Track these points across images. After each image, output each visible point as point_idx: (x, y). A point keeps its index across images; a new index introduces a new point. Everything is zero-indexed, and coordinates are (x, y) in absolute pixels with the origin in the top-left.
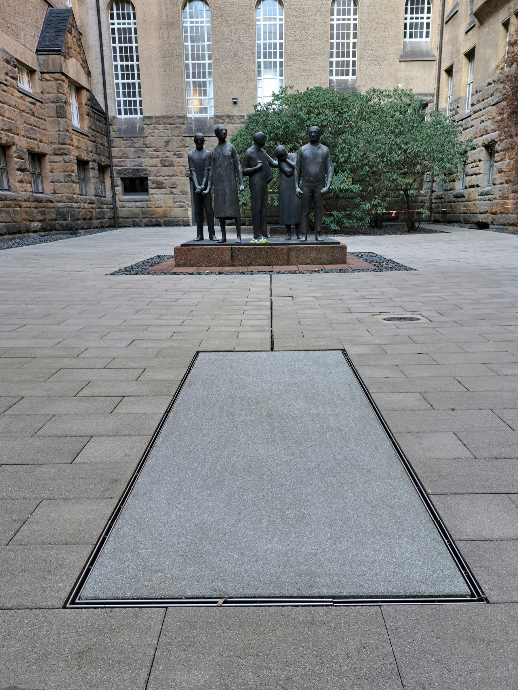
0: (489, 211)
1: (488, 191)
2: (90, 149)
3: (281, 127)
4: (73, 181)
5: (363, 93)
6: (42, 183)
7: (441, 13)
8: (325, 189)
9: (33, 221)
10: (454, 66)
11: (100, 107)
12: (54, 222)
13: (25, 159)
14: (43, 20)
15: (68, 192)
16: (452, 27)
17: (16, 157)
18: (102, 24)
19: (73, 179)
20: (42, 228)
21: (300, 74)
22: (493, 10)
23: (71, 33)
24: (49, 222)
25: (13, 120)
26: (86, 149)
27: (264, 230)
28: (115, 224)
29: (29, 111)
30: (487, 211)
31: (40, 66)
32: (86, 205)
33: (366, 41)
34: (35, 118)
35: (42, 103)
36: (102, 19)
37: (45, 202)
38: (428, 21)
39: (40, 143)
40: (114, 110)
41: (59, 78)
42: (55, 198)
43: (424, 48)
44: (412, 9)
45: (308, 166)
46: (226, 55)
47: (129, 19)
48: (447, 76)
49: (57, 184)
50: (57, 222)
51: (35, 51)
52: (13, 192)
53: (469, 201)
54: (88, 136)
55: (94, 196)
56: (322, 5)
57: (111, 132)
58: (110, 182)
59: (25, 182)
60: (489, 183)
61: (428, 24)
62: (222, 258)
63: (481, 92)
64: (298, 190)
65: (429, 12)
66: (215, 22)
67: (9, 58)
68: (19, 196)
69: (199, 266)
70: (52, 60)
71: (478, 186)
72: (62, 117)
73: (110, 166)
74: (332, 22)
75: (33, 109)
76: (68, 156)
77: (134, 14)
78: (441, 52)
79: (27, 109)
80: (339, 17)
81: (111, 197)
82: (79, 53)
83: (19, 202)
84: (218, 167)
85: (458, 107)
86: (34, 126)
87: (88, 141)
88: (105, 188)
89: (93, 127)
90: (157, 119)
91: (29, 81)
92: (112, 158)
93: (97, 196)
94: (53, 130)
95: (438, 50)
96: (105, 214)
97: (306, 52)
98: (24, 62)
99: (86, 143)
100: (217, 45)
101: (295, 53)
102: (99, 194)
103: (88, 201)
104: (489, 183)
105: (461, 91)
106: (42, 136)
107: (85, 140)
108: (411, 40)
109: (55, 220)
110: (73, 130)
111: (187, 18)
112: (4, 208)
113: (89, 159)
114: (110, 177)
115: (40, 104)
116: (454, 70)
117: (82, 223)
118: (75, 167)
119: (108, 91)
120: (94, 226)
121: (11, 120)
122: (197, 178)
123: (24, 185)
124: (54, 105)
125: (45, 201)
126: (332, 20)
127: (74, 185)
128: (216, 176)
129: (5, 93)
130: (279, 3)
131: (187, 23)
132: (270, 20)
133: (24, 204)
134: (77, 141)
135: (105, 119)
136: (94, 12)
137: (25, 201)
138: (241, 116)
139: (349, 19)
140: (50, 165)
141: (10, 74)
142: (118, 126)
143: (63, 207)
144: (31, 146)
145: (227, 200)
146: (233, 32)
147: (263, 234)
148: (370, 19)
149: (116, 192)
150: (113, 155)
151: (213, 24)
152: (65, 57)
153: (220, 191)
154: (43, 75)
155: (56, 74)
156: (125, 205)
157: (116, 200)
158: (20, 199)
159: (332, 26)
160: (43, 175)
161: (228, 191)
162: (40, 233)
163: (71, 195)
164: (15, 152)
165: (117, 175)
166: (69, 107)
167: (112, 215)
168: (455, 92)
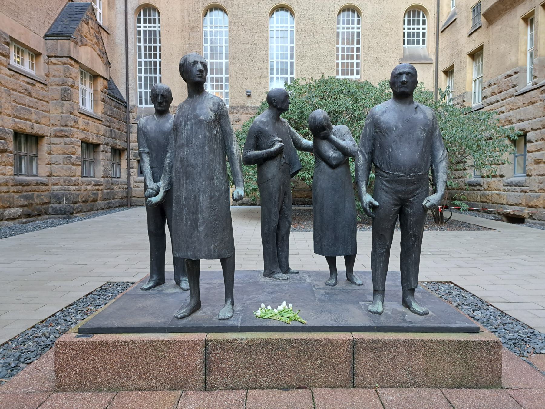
0: (523, 204)
1: (519, 182)
2: (102, 132)
3: (296, 112)
4: (73, 163)
5: (376, 85)
6: (37, 165)
7: (436, 24)
8: (433, 199)
9: (9, 207)
10: (455, 66)
11: (122, 97)
12: (46, 206)
13: (7, 139)
14: (60, 10)
15: (66, 174)
16: (449, 34)
18: (128, 26)
19: (72, 161)
20: (25, 214)
21: (309, 73)
22: (508, 7)
23: (87, 24)
24: (38, 207)
26: (95, 132)
27: (284, 260)
28: (128, 203)
29: (23, 91)
30: (520, 204)
31: (47, 51)
32: (89, 187)
33: (369, 46)
34: (32, 99)
35: (46, 85)
36: (129, 22)
38: (424, 31)
39: (35, 124)
40: (134, 100)
41: (66, 62)
42: (51, 181)
43: (422, 53)
44: (409, 21)
45: (394, 146)
46: (242, 55)
47: (155, 23)
48: (445, 76)
49: (55, 166)
50: (50, 205)
51: (43, 35)
53: (490, 191)
54: (101, 121)
55: (103, 177)
56: (329, 16)
57: (131, 119)
58: (126, 164)
59: (3, 164)
60: (514, 173)
61: (424, 34)
62: (181, 367)
63: (496, 85)
64: (367, 198)
65: (424, 23)
66: (233, 27)
69: (117, 391)
70: (61, 45)
71: (502, 176)
72: (66, 99)
73: (127, 149)
74: (338, 30)
75: (30, 89)
77: (159, 19)
78: (438, 56)
79: (21, 88)
80: (344, 26)
81: (125, 178)
82: (98, 44)
84: (182, 146)
85: (464, 101)
86: (29, 106)
87: (100, 126)
88: (120, 170)
89: (109, 113)
90: (175, 109)
91: (33, 64)
92: (130, 143)
93: (107, 177)
94: (55, 112)
95: (435, 55)
96: (116, 195)
97: (315, 54)
98: (23, 42)
99: (97, 127)
100: (234, 46)
101: (304, 54)
102: (109, 176)
103: (93, 183)
104: (514, 173)
105: (467, 87)
106: (40, 118)
107: (96, 124)
108: (409, 46)
109: (49, 203)
110: (80, 113)
111: (207, 24)
113: (99, 142)
114: (127, 159)
115: (42, 86)
116: (455, 69)
117: (81, 206)
118: (79, 150)
119: (130, 82)
120: (99, 207)
122: (152, 168)
124: (59, 88)
125: (35, 184)
126: (338, 28)
127: (74, 167)
128: (178, 165)
130: (291, 14)
131: (207, 27)
132: (282, 27)
134: (85, 124)
135: (126, 107)
136: (123, 16)
138: (254, 107)
139: (353, 28)
140: (47, 147)
142: (138, 114)
143: (58, 190)
144: (19, 126)
145: (201, 220)
146: (248, 36)
147: (281, 267)
148: (372, 27)
149: (131, 174)
150: (131, 139)
151: (230, 29)
152: (76, 43)
153: (186, 199)
154: (49, 59)
155: (64, 58)
156: (139, 186)
157: (130, 181)
159: (338, 33)
161: (204, 201)
162: (20, 220)
163: (69, 178)
165: (134, 158)
166: (77, 90)
167: (125, 195)
168: (459, 89)
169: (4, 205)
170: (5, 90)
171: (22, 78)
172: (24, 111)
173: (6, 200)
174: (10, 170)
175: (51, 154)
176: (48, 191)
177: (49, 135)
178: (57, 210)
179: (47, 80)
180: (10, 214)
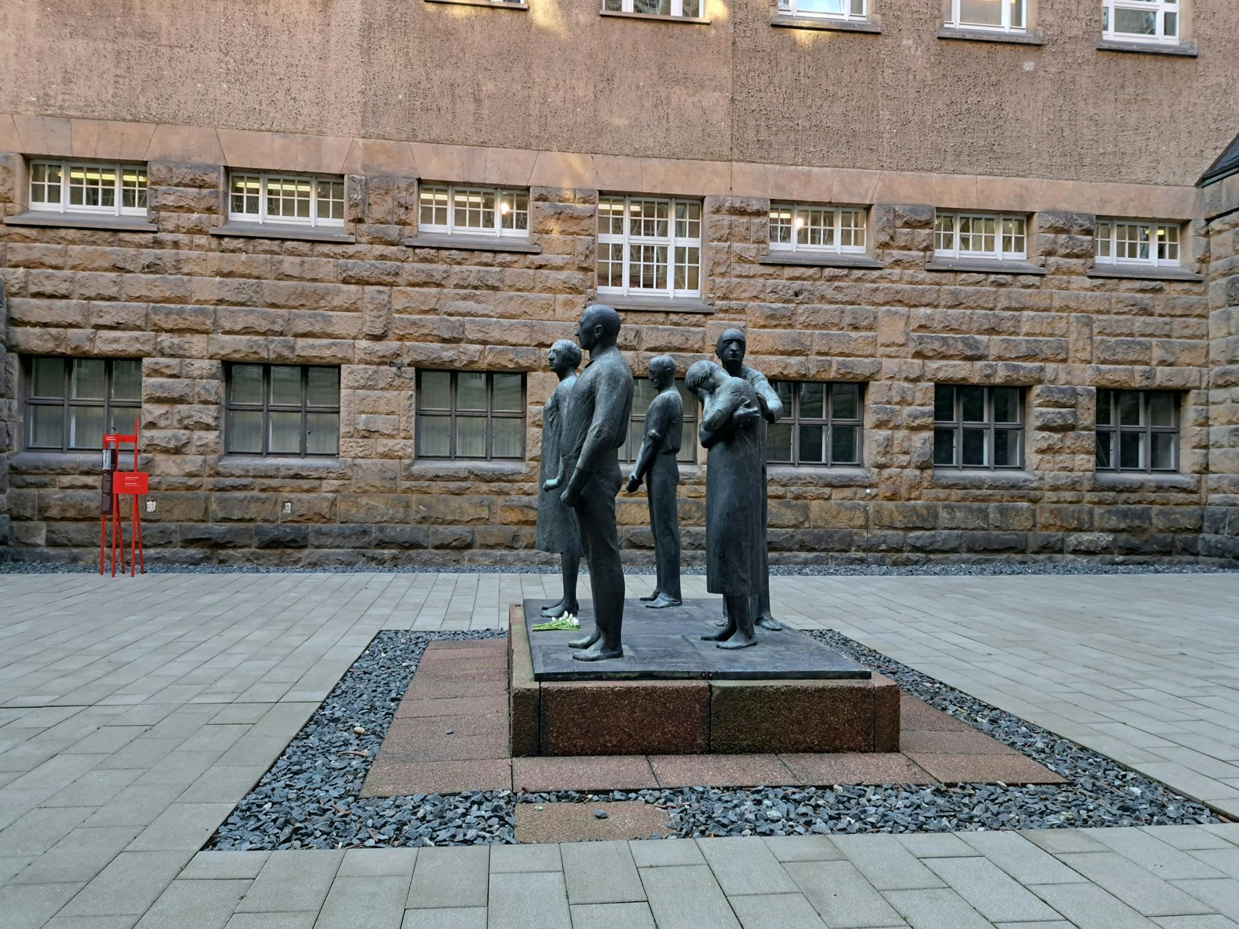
17: (1040, 405)
24: (1161, 536)
25: (1052, 335)
29: (1126, 309)
34: (1149, 319)
37: (1154, 492)
39: (1159, 368)
50: (1201, 536)
52: (1028, 472)
59: (1067, 451)
67: (1060, 224)
68: (1033, 478)
83: (1032, 492)
106: (1173, 353)
112: (968, 503)
115: (1186, 286)
121: (1044, 335)
123: (1059, 458)
124: (1223, 281)
129: (1030, 290)
133: (1052, 496)
137: (1055, 489)
141: (1062, 251)
143: (1218, 502)
144: (1111, 378)
158: (1034, 485)
160: (1182, 433)
162: (1108, 557)
164: (1038, 395)
169: (1066, 525)
170: (1077, 318)
171: (1125, 285)
172: (1125, 347)
173: (1073, 517)
174: (1085, 462)
175: (1210, 426)
176: (1196, 504)
177: (1204, 384)
178: (1210, 547)
179: (1204, 272)
180: (1080, 543)
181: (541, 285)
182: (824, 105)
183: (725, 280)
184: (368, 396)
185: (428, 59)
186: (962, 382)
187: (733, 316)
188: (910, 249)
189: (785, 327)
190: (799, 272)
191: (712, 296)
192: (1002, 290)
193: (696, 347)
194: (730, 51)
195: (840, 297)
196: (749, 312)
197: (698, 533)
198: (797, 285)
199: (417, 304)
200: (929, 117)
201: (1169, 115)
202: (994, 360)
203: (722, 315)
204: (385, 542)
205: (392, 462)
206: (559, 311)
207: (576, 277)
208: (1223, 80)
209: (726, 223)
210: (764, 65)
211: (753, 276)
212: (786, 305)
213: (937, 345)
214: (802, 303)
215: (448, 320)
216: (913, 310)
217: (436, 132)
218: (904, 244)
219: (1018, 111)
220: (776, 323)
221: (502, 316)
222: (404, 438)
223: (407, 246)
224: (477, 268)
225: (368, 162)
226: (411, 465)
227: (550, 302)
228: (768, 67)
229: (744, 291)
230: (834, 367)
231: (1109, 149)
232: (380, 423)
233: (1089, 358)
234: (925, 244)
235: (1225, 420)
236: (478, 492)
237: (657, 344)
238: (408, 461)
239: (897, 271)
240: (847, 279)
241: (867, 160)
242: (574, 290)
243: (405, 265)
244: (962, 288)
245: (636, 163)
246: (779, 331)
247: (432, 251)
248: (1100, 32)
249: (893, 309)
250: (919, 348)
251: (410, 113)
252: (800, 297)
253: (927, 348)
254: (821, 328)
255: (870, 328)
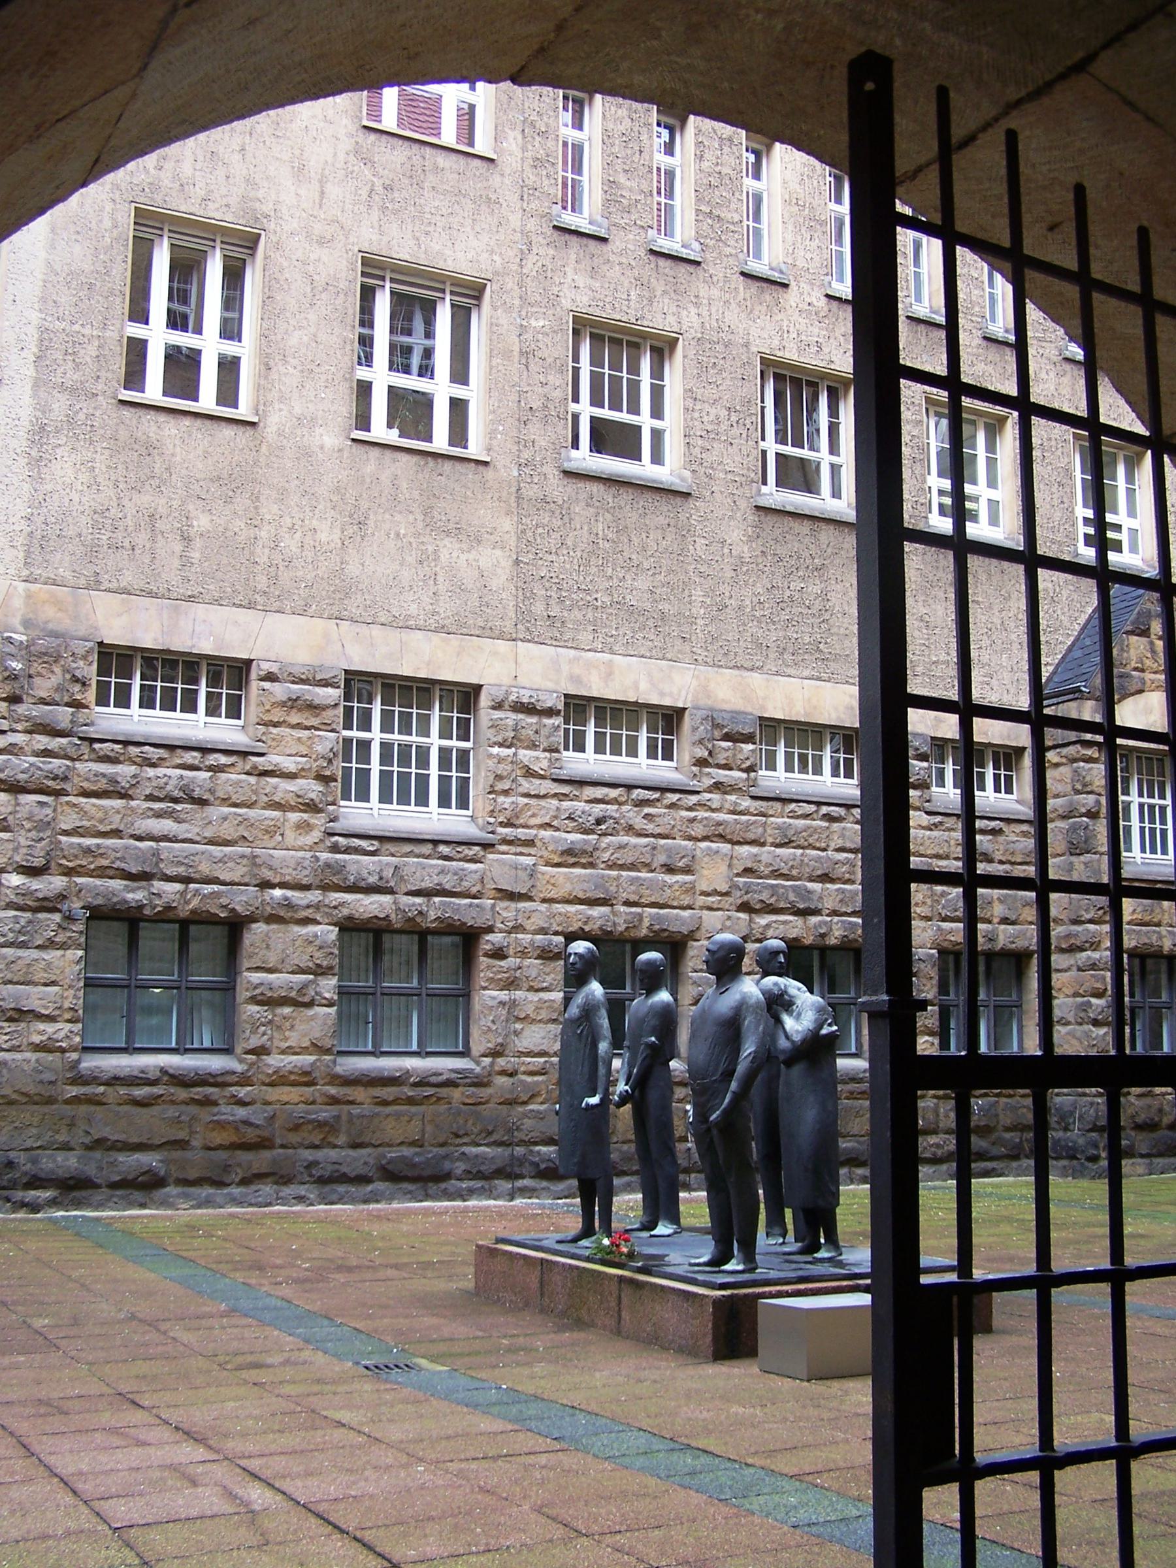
39: (1002, 927)
76: (1084, 954)
181: (266, 799)
182: (627, 577)
183: (509, 800)
184: (20, 958)
185: (121, 479)
186: (795, 944)
187: (519, 849)
188: (731, 769)
189: (584, 866)
190: (600, 792)
191: (492, 820)
192: (836, 826)
193: (474, 890)
194: (513, 499)
195: (650, 828)
196: (539, 844)
197: (477, 1156)
198: (598, 810)
199: (93, 822)
200: (748, 602)
201: (999, 622)
202: (827, 915)
203: (504, 848)
204: (40, 1179)
205: (50, 1057)
206: (291, 837)
207: (312, 789)
208: (1050, 585)
209: (510, 722)
210: (554, 520)
211: (545, 796)
212: (585, 837)
213: (764, 896)
214: (605, 834)
215: (137, 848)
216: (736, 847)
217: (128, 578)
218: (724, 762)
219: (845, 605)
220: (572, 860)
221: (211, 842)
222: (69, 1021)
223: (80, 738)
224: (179, 772)
225: (31, 615)
226: (78, 1061)
227: (278, 824)
228: (560, 523)
229: (533, 815)
230: (646, 923)
231: (941, 658)
232: (35, 998)
233: (929, 914)
234: (748, 763)
235: (1069, 991)
236: (173, 1102)
237: (424, 885)
238: (74, 1056)
239: (715, 798)
240: (658, 804)
241: (680, 652)
242: (312, 807)
243: (78, 765)
244: (791, 821)
245: (394, 635)
246: (578, 871)
247: (117, 747)
248: (926, 518)
249: (714, 845)
250: (745, 898)
251: (92, 551)
252: (603, 827)
253: (754, 898)
254: (629, 869)
255: (687, 871)
